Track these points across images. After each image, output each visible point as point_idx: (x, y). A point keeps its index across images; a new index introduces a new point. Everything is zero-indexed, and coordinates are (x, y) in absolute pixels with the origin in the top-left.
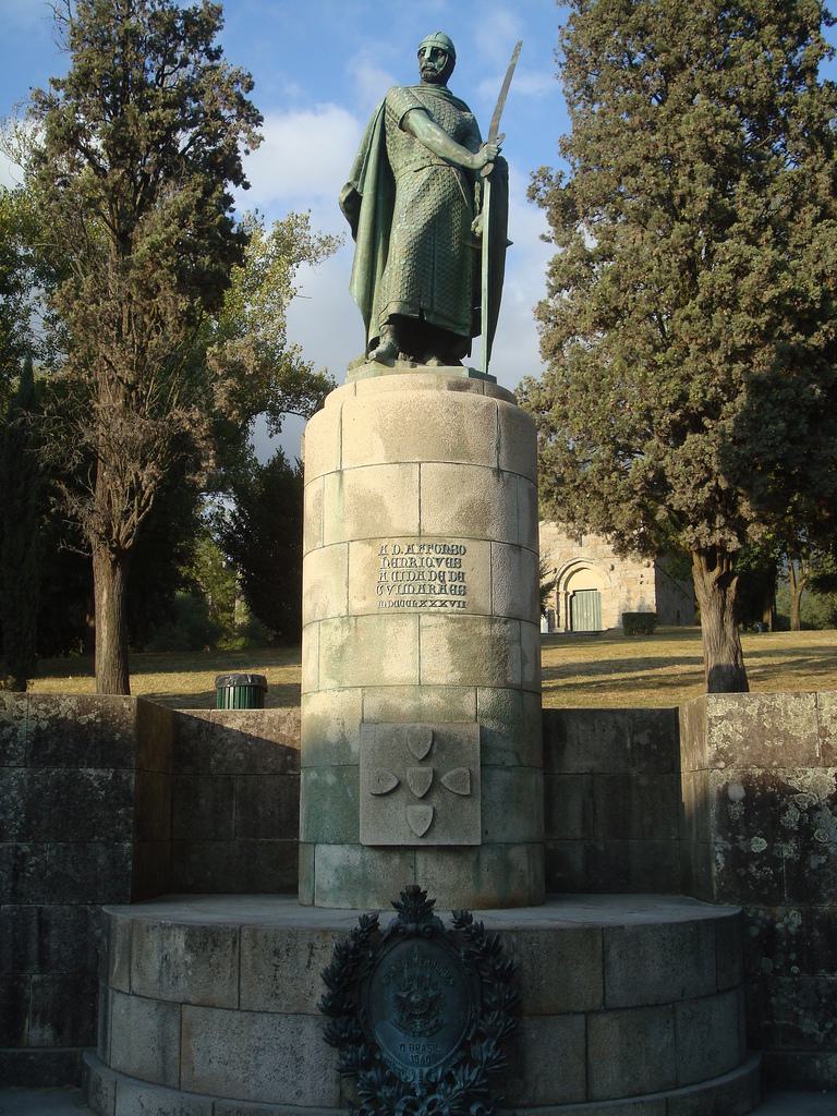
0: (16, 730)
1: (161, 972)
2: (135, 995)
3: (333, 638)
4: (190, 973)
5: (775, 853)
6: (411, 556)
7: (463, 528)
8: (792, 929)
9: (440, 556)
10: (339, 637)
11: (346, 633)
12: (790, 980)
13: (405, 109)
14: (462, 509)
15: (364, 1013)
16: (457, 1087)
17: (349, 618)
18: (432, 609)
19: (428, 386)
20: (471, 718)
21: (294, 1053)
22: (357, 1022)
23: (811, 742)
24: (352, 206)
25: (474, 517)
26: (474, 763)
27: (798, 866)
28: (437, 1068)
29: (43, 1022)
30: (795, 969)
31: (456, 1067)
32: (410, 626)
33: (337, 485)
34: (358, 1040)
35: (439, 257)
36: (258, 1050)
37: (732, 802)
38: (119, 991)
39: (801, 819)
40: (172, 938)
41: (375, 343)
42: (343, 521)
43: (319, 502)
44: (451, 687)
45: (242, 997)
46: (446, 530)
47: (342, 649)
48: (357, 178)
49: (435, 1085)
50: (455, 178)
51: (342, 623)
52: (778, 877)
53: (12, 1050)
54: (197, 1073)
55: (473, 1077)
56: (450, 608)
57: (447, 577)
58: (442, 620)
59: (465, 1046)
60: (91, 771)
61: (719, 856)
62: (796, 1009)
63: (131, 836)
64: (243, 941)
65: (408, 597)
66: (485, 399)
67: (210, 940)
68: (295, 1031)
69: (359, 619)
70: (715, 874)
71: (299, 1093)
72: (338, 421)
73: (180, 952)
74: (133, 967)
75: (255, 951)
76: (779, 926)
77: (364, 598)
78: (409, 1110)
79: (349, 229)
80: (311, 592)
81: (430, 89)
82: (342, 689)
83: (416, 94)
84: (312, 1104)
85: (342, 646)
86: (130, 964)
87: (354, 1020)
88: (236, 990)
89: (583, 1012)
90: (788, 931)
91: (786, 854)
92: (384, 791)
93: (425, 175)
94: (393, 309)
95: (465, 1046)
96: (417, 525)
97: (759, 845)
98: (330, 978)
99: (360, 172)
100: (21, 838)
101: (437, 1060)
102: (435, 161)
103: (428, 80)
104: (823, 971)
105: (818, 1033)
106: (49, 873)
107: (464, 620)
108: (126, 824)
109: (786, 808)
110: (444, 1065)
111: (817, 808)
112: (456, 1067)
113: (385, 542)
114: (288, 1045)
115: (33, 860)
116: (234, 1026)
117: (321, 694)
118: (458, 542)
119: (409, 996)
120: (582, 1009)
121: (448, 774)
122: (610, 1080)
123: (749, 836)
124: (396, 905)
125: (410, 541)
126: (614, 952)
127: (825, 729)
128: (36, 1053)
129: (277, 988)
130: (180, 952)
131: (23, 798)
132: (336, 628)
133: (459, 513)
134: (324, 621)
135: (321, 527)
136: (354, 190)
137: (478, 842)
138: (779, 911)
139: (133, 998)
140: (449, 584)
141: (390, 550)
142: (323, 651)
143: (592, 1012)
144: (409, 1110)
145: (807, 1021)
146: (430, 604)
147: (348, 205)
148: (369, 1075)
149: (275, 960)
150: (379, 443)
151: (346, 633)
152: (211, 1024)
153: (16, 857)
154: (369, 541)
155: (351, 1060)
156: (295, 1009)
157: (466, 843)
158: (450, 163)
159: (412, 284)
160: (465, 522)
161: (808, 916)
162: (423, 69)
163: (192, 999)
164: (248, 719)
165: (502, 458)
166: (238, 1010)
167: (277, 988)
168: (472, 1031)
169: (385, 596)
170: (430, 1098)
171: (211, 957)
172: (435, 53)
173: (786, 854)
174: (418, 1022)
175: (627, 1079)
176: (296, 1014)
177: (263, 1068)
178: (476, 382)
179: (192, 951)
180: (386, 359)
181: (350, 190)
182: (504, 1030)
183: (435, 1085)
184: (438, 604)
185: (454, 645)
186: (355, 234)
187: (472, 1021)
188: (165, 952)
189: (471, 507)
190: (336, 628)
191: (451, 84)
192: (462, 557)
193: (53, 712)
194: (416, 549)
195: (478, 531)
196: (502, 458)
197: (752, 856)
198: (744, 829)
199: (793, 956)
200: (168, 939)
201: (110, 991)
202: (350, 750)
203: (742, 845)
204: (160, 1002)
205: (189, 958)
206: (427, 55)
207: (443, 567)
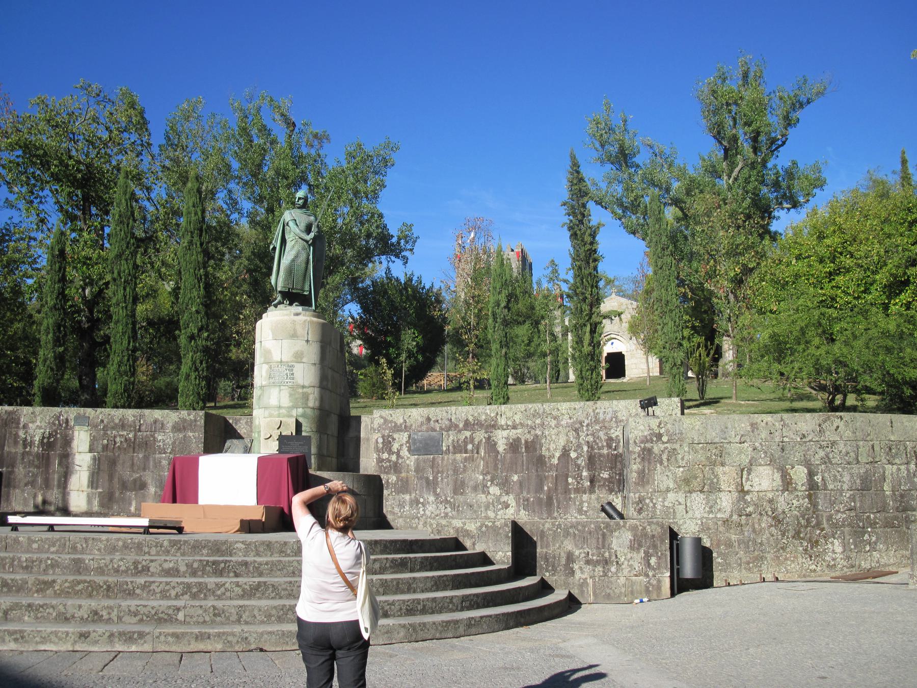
17: (262, 387)
19: (287, 315)
23: (401, 425)
25: (298, 357)
27: (396, 464)
32: (277, 389)
44: (288, 408)
82: (260, 408)
97: (385, 456)
123: (383, 453)
138: (389, 476)
154: (267, 363)
160: (295, 357)
185: (291, 395)
195: (299, 360)
196: (310, 336)
197: (383, 460)
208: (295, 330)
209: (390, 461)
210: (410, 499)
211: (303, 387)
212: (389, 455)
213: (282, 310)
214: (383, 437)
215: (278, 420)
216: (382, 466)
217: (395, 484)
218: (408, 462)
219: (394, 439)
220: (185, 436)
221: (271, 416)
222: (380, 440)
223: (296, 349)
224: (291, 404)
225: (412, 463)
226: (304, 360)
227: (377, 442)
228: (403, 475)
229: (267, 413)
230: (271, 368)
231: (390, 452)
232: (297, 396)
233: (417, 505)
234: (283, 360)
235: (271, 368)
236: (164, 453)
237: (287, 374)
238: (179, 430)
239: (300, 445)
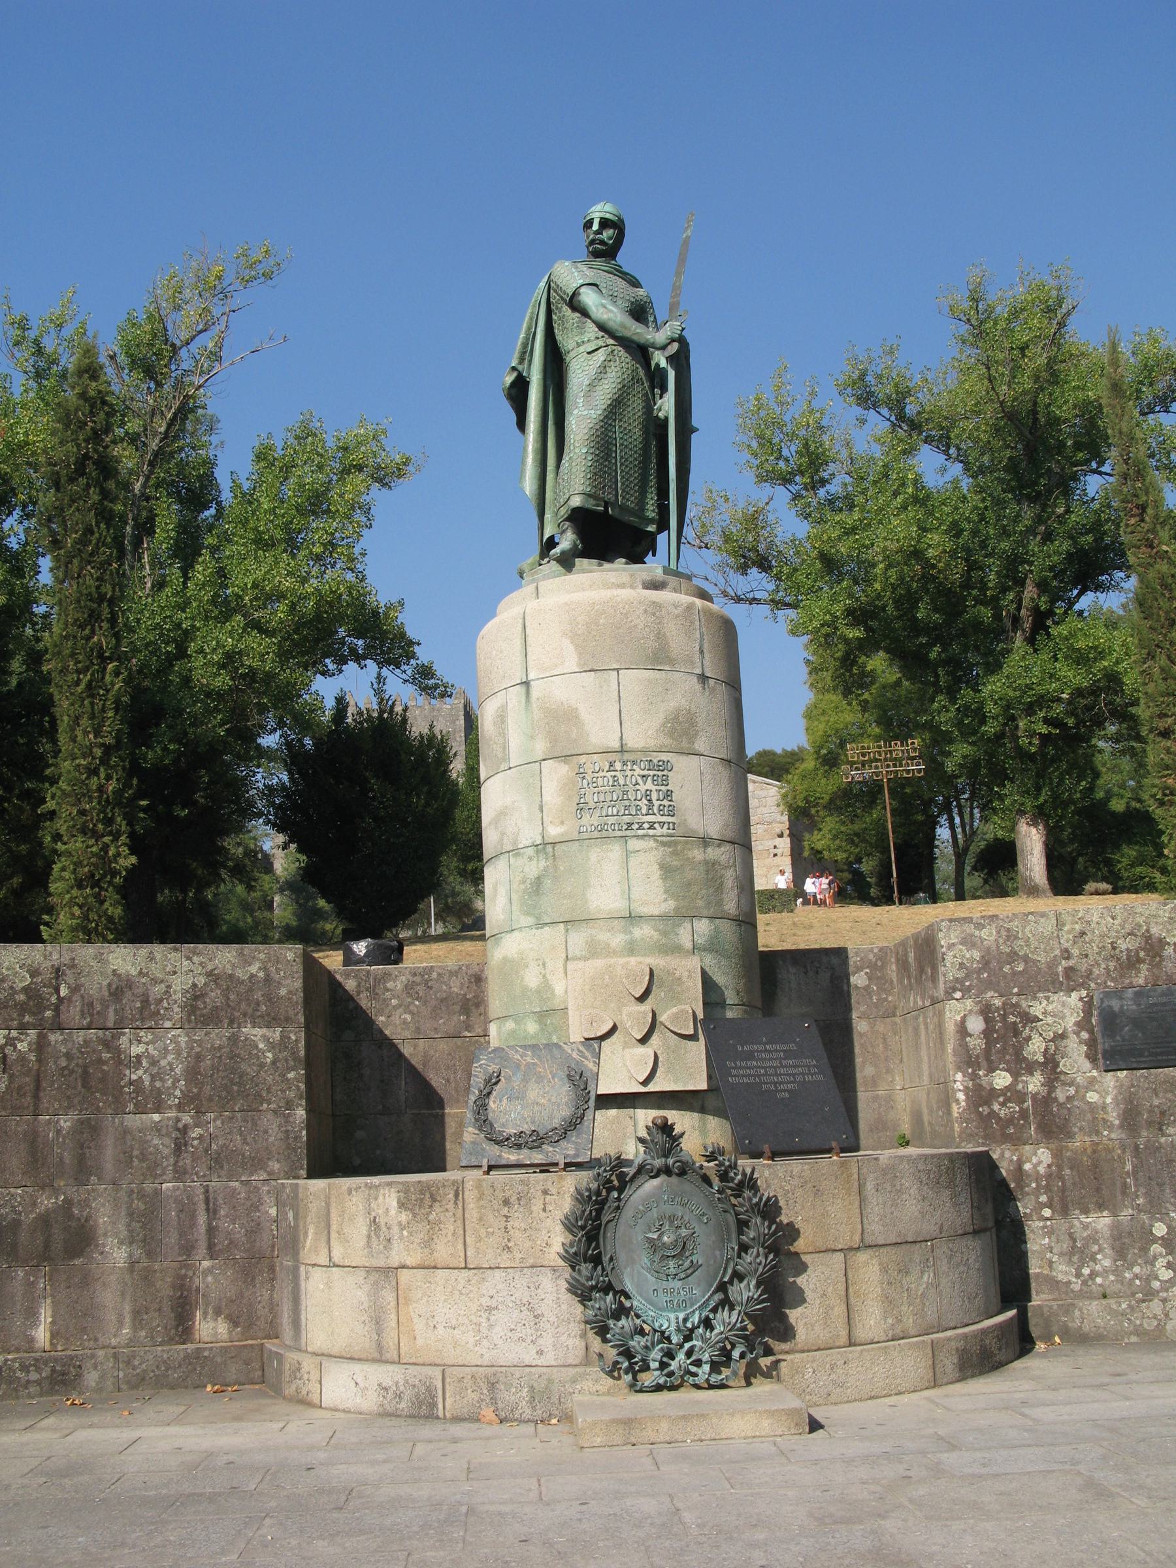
0: (169, 987)
1: (369, 1237)
2: (338, 1266)
3: (527, 869)
4: (405, 1233)
5: (1020, 1086)
6: (613, 773)
7: (668, 741)
8: (1042, 1170)
9: (646, 772)
10: (533, 868)
11: (543, 864)
12: (1041, 1224)
13: (575, 285)
15: (611, 1259)
16: (716, 1331)
17: (545, 846)
18: (640, 832)
19: (622, 586)
20: (688, 951)
21: (531, 1310)
22: (603, 1270)
24: (518, 392)
26: (696, 999)
27: (1045, 1102)
28: (694, 1312)
29: (218, 1312)
30: (1047, 1212)
31: (714, 1310)
32: (615, 851)
33: (524, 698)
34: (607, 1288)
35: (621, 445)
36: (490, 1309)
37: (971, 1036)
38: (314, 1265)
39: (1046, 1049)
40: (381, 1197)
41: (551, 543)
43: (502, 718)
44: (663, 917)
45: (469, 1253)
46: (652, 743)
47: (538, 881)
48: (521, 361)
49: (692, 1330)
51: (537, 852)
52: (1024, 1114)
53: (185, 1346)
54: (420, 1342)
55: (733, 1320)
56: (659, 831)
57: (654, 796)
58: (652, 844)
59: (722, 1287)
60: (258, 1032)
61: (961, 1096)
62: (1049, 1255)
63: (303, 1102)
64: (467, 1193)
65: (612, 820)
66: (685, 599)
67: (428, 1195)
68: (532, 1285)
69: (558, 846)
70: (956, 1115)
71: (540, 1353)
73: (393, 1212)
74: (334, 1235)
75: (482, 1202)
76: (1027, 1167)
77: (562, 823)
78: (665, 1359)
79: (513, 417)
80: (496, 821)
82: (540, 925)
84: (553, 1363)
85: (538, 878)
86: (329, 1233)
87: (600, 1268)
88: (460, 1247)
89: (841, 1250)
90: (1038, 1172)
91: (1031, 1088)
92: (599, 1034)
93: (601, 356)
94: (576, 502)
95: (722, 1287)
96: (618, 739)
97: (1002, 1079)
98: (570, 1225)
99: (526, 354)
100: (180, 1108)
101: (692, 1305)
102: (611, 341)
104: (1077, 1212)
105: (1074, 1280)
106: (214, 1147)
107: (676, 843)
108: (298, 1088)
109: (1029, 1038)
110: (701, 1308)
111: (1063, 1036)
112: (714, 1310)
113: (583, 759)
114: (525, 1301)
115: (197, 1132)
116: (460, 1287)
117: (516, 934)
118: (664, 757)
119: (660, 1236)
120: (840, 1247)
121: (669, 1012)
122: (872, 1322)
123: (991, 1070)
124: (642, 1140)
125: (612, 757)
126: (870, 1186)
127: (1067, 950)
128: (211, 1349)
129: (509, 1240)
130: (393, 1212)
131: (182, 1063)
132: (530, 859)
133: (664, 725)
134: (515, 851)
135: (505, 747)
137: (703, 1086)
139: (334, 1269)
140: (656, 803)
141: (589, 768)
142: (515, 886)
143: (851, 1249)
144: (665, 1359)
145: (1063, 1267)
146: (637, 826)
147: (513, 391)
148: (620, 1324)
149: (505, 1211)
150: (569, 649)
151: (543, 864)
152: (433, 1286)
153: (178, 1130)
154: (565, 758)
155: (600, 1309)
156: (531, 1261)
157: (691, 1088)
158: (625, 342)
160: (671, 734)
161: (1057, 1155)
163: (409, 1261)
164: (415, 975)
165: (707, 663)
166: (466, 1268)
167: (509, 1240)
168: (730, 1271)
169: (586, 819)
170: (687, 1346)
171: (428, 1214)
173: (1031, 1088)
174: (672, 1263)
175: (890, 1321)
176: (532, 1267)
177: (497, 1329)
178: (673, 581)
179: (406, 1209)
180: (566, 562)
181: (515, 374)
182: (765, 1266)
183: (692, 1330)
184: (646, 826)
185: (667, 871)
186: (522, 424)
187: (728, 1260)
188: (373, 1214)
189: (676, 718)
190: (530, 859)
191: (622, 257)
192: (670, 774)
193: (210, 967)
194: (618, 766)
195: (685, 744)
196: (707, 663)
197: (993, 1093)
198: (984, 1064)
199: (1043, 1198)
200: (376, 1199)
201: (302, 1268)
202: (553, 993)
203: (984, 1081)
204: (370, 1270)
205: (404, 1217)
206: (595, 227)
207: (649, 785)
208: (660, 636)
209: (1021, 1097)
210: (1115, 1227)
211: (705, 841)
212: (1016, 1075)
213: (583, 571)
214: (986, 1011)
215: (640, 963)
216: (993, 1114)
217: (1049, 1176)
218: (1092, 1097)
219: (1032, 1020)
220: (234, 1039)
221: (594, 951)
222: (976, 1025)
223: (673, 704)
224: (670, 905)
225: (1109, 1100)
226: (701, 745)
227: (963, 1031)
228: (1079, 1142)
229: (578, 940)
230: (581, 775)
231: (1020, 1066)
232: (689, 875)
233: (1145, 1250)
234: (631, 743)
235: (581, 775)
236: (158, 1109)
237: (647, 794)
238: (211, 1019)
239: (788, 1054)
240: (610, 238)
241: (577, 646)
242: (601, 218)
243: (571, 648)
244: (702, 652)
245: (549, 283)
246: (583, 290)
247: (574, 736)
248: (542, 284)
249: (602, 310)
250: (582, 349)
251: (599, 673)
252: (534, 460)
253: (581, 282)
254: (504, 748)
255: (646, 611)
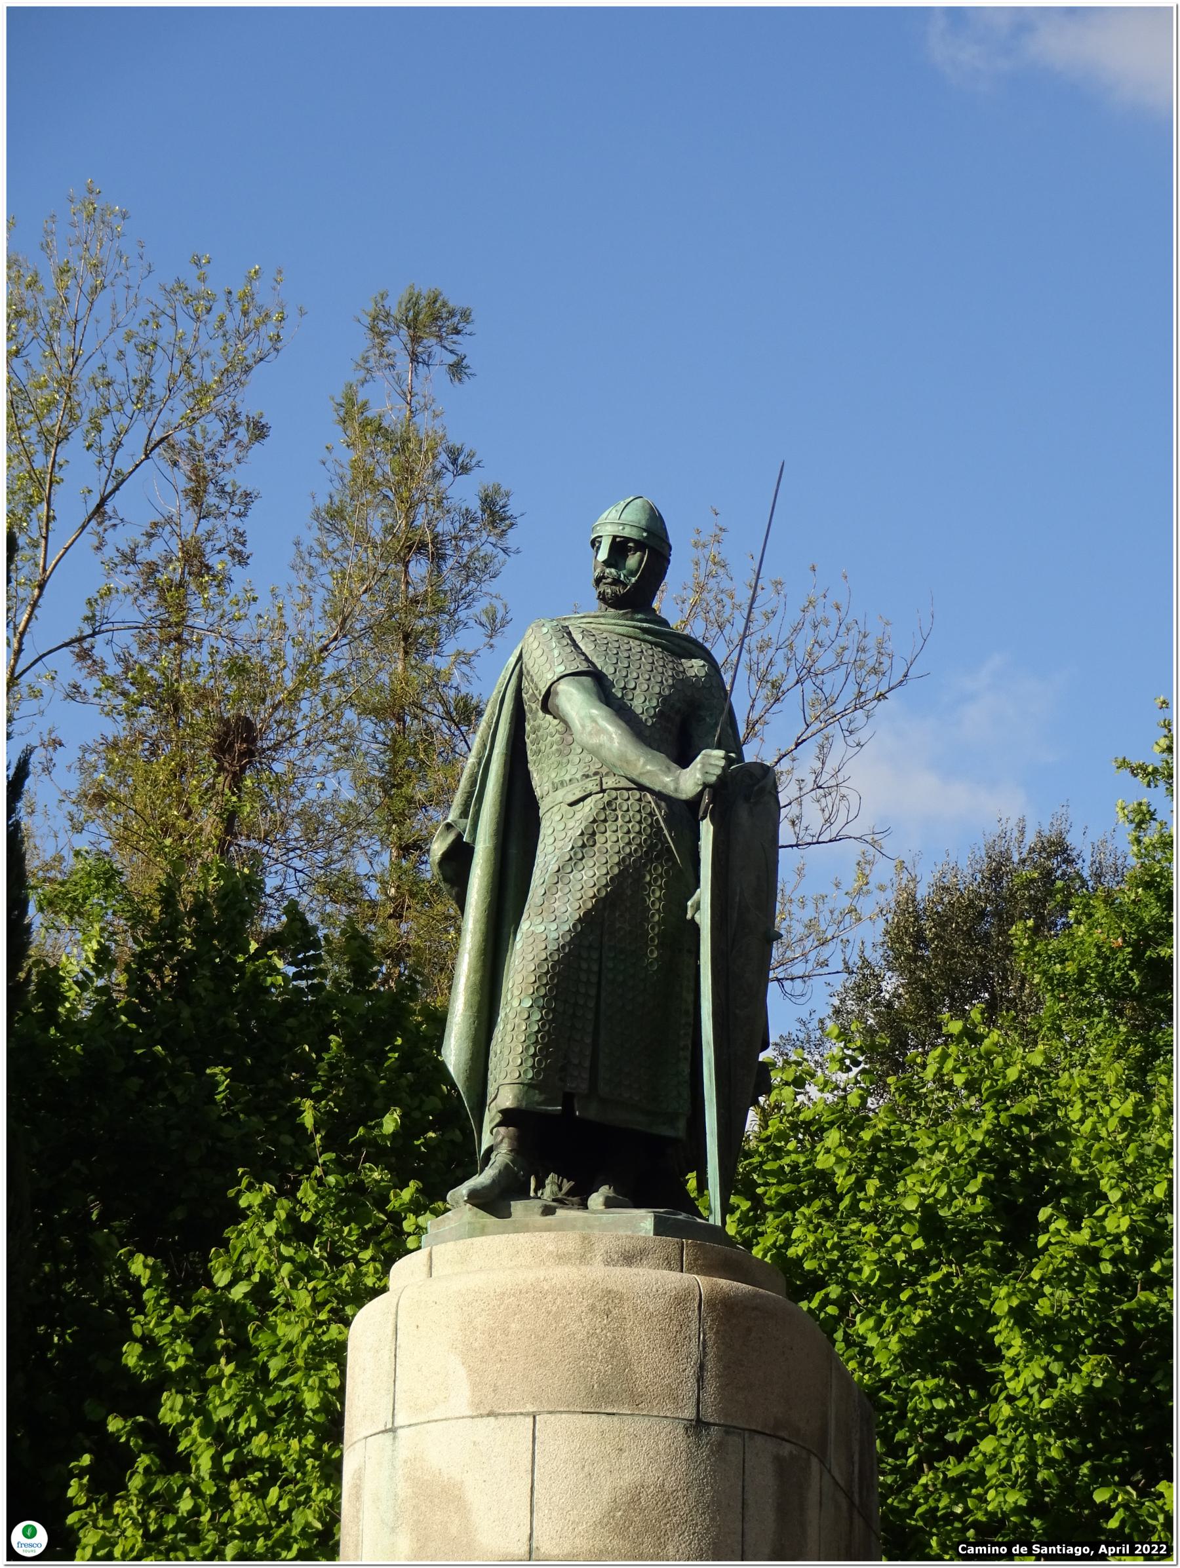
13: (550, 677)
14: (615, 1505)
42: (393, 1530)
48: (464, 814)
50: (651, 814)
72: (391, 1328)
81: (613, 624)
83: (577, 637)
103: (614, 602)
133: (610, 1513)
136: (460, 836)
159: (545, 1047)
160: (621, 1531)
162: (598, 581)
172: (620, 548)
181: (451, 837)
189: (635, 1500)
206: (603, 555)
223: (628, 1478)
240: (632, 573)
241: (471, 1370)
242: (615, 537)
243: (462, 1372)
244: (700, 1379)
245: (520, 658)
246: (563, 687)
247: (454, 1530)
248: (513, 660)
249: (589, 726)
250: (560, 794)
251: (502, 1420)
252: (469, 1005)
253: (560, 670)
254: (357, 1546)
255: (592, 1308)
